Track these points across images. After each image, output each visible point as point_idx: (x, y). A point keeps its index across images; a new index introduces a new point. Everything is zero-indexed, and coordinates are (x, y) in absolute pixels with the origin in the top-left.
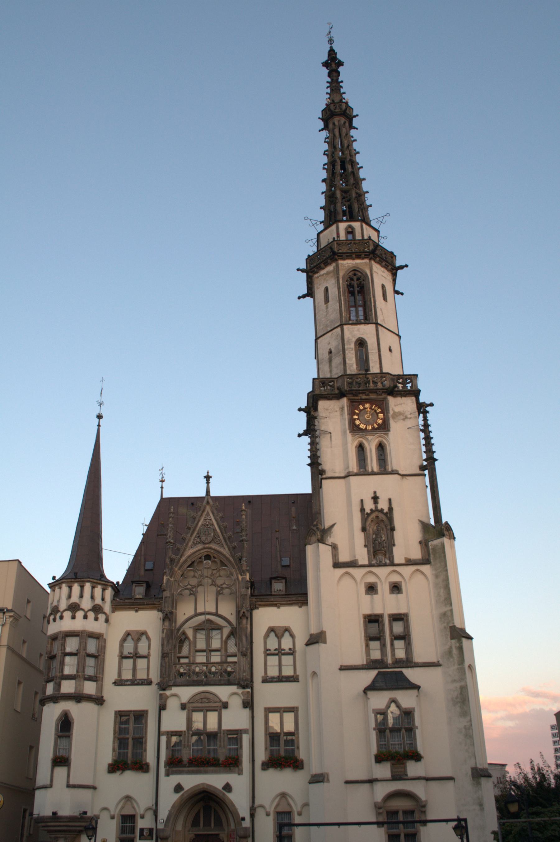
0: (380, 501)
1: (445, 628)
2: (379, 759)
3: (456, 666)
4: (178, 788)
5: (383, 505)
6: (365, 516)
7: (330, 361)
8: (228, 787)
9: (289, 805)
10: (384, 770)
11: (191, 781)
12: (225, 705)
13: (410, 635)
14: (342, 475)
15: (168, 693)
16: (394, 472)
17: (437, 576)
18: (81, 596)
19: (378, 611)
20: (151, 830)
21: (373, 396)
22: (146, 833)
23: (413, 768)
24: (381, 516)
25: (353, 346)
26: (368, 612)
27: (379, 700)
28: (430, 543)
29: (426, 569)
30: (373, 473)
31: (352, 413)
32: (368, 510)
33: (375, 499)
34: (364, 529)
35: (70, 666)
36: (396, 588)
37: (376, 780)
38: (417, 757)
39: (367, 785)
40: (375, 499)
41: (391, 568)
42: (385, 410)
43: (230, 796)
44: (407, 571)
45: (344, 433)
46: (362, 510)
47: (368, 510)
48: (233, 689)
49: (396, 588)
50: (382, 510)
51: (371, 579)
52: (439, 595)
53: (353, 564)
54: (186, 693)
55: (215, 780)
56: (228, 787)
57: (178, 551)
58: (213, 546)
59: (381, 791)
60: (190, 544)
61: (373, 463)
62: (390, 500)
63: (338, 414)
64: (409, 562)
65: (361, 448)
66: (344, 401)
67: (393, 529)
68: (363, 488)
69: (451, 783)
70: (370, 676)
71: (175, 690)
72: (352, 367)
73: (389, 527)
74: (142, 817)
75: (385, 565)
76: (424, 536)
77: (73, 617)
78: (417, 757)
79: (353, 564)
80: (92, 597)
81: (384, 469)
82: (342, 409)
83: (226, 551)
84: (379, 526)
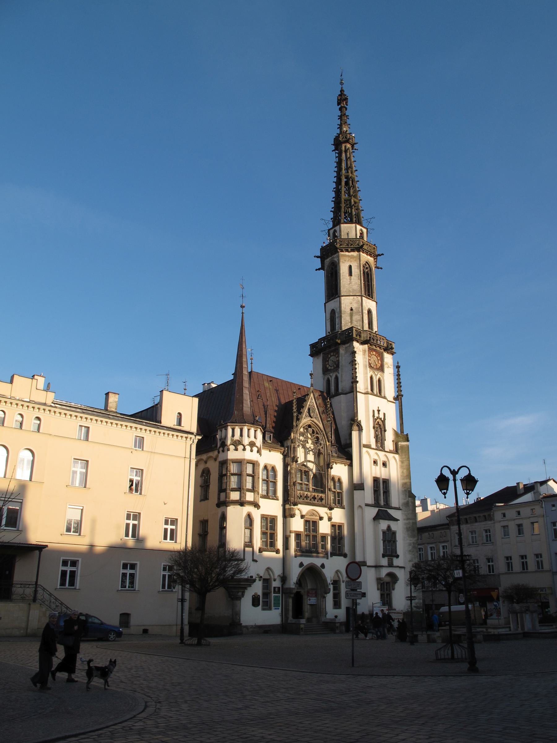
0: (380, 412)
1: (405, 490)
2: (384, 556)
3: (411, 512)
4: (301, 565)
5: (381, 416)
6: (375, 420)
7: (351, 316)
8: (323, 566)
9: (338, 576)
10: (385, 562)
11: (307, 561)
12: (321, 518)
13: (389, 491)
14: (363, 392)
15: (295, 507)
16: (385, 398)
17: (402, 462)
18: (241, 435)
19: (378, 476)
20: (279, 588)
21: (378, 349)
22: (276, 589)
23: (396, 562)
24: (381, 423)
25: (366, 312)
26: (375, 476)
27: (384, 525)
28: (399, 443)
29: (397, 456)
30: (376, 396)
31: (369, 356)
32: (376, 417)
33: (379, 411)
34: (374, 428)
35: (233, 481)
36: (384, 464)
37: (382, 566)
38: (397, 556)
39: (373, 569)
40: (379, 411)
41: (383, 453)
42: (382, 359)
43: (324, 571)
44: (391, 456)
45: (365, 366)
46: (374, 416)
47: (376, 417)
48: (326, 510)
49: (384, 464)
50: (381, 419)
51: (376, 457)
52: (403, 472)
53: (368, 446)
54: (305, 509)
55: (317, 561)
56: (323, 566)
57: (298, 419)
58: (315, 421)
59: (384, 572)
60: (304, 416)
61: (376, 390)
62: (384, 414)
63: (362, 353)
64: (390, 452)
65: (371, 378)
66: (366, 346)
67: (385, 431)
68: (375, 402)
69: (403, 569)
70: (375, 511)
71: (300, 506)
72: (366, 327)
73: (383, 429)
74: (275, 580)
75: (381, 450)
76: (395, 438)
77: (252, 451)
78: (397, 556)
79: (368, 446)
80: (248, 436)
81: (380, 394)
82: (364, 351)
83: (321, 425)
84: (380, 427)
